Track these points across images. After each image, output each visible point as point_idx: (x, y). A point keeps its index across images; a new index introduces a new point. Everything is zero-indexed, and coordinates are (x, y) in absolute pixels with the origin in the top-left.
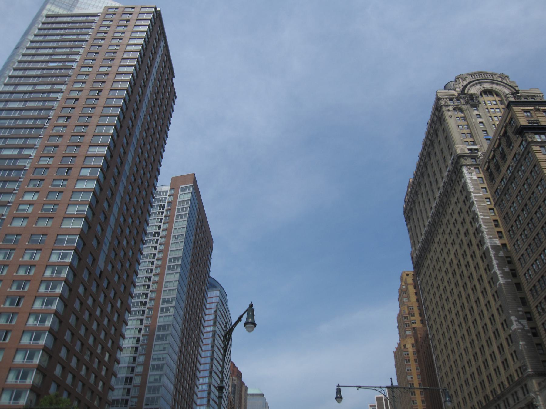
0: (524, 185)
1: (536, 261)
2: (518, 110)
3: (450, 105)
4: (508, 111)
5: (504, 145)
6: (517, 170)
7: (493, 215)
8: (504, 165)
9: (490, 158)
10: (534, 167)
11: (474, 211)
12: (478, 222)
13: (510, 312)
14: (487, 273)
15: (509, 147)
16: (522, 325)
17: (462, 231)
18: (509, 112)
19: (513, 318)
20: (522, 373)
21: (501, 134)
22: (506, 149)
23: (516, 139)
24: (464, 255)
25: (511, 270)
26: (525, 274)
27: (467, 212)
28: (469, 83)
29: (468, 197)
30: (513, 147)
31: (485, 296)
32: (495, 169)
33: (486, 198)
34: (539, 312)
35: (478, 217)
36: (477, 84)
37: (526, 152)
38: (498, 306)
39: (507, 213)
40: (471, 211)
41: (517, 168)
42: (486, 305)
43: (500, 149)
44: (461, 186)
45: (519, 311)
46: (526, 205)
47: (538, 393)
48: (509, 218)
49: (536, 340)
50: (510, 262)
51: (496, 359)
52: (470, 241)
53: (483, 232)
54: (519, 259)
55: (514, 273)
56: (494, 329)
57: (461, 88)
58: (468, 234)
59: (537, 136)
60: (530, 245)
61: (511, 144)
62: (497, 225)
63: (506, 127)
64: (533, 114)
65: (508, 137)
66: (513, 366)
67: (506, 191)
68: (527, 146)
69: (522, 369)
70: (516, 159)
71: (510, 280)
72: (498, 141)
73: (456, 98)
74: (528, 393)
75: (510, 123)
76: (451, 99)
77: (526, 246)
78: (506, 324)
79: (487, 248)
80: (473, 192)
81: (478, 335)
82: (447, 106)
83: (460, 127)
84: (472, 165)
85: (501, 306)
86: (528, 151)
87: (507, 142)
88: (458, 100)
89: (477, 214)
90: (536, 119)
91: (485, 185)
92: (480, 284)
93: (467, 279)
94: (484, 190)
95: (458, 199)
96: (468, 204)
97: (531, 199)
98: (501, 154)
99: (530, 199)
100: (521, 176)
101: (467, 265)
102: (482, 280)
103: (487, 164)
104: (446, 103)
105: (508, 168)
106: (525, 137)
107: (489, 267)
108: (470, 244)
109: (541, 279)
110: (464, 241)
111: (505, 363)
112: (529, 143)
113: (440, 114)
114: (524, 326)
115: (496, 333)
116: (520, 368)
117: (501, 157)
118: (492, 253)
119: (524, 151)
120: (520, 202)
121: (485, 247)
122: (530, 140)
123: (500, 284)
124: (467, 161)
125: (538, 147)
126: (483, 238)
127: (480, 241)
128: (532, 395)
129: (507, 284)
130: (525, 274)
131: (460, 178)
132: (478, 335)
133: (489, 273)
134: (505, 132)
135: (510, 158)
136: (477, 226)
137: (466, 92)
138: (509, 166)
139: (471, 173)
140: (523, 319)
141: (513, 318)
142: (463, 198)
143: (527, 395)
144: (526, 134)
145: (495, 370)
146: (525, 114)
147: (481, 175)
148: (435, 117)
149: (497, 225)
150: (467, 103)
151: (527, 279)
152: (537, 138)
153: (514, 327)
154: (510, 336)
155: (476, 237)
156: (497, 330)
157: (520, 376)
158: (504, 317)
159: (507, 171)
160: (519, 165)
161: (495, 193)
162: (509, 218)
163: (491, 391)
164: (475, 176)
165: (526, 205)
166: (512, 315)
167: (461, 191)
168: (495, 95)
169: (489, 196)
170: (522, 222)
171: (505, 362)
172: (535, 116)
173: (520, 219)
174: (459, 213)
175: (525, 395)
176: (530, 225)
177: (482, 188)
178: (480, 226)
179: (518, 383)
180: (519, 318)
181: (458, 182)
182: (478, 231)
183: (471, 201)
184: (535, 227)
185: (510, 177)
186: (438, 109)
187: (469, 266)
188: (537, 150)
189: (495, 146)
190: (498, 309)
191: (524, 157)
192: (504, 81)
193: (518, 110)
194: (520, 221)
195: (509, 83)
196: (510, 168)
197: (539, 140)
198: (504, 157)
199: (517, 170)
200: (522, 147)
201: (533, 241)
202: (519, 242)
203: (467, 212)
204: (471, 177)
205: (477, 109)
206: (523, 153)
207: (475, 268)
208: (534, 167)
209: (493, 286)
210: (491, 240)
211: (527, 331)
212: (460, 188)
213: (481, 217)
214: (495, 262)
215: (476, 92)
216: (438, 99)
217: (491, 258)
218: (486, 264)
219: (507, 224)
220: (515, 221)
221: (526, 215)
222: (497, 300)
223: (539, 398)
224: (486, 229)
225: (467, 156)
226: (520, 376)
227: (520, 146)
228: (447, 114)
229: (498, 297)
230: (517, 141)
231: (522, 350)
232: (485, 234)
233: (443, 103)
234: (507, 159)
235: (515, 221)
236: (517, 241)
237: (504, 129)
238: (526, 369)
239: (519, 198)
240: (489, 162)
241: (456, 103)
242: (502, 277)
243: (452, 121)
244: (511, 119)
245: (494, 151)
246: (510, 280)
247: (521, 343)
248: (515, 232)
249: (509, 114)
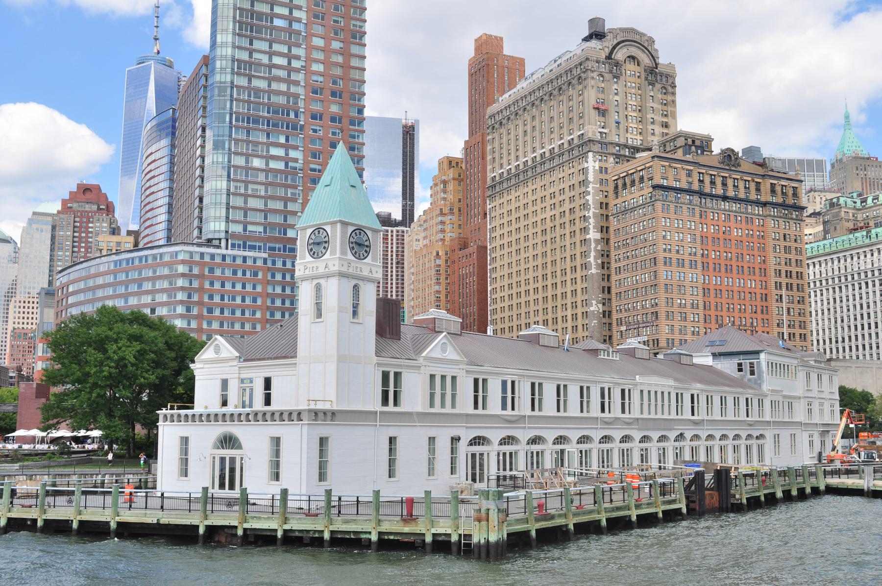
19: (594, 302)
80: (593, 183)
118: (593, 245)
121: (588, 237)
141: (594, 302)
180: (598, 302)
214: (593, 254)
232: (591, 227)
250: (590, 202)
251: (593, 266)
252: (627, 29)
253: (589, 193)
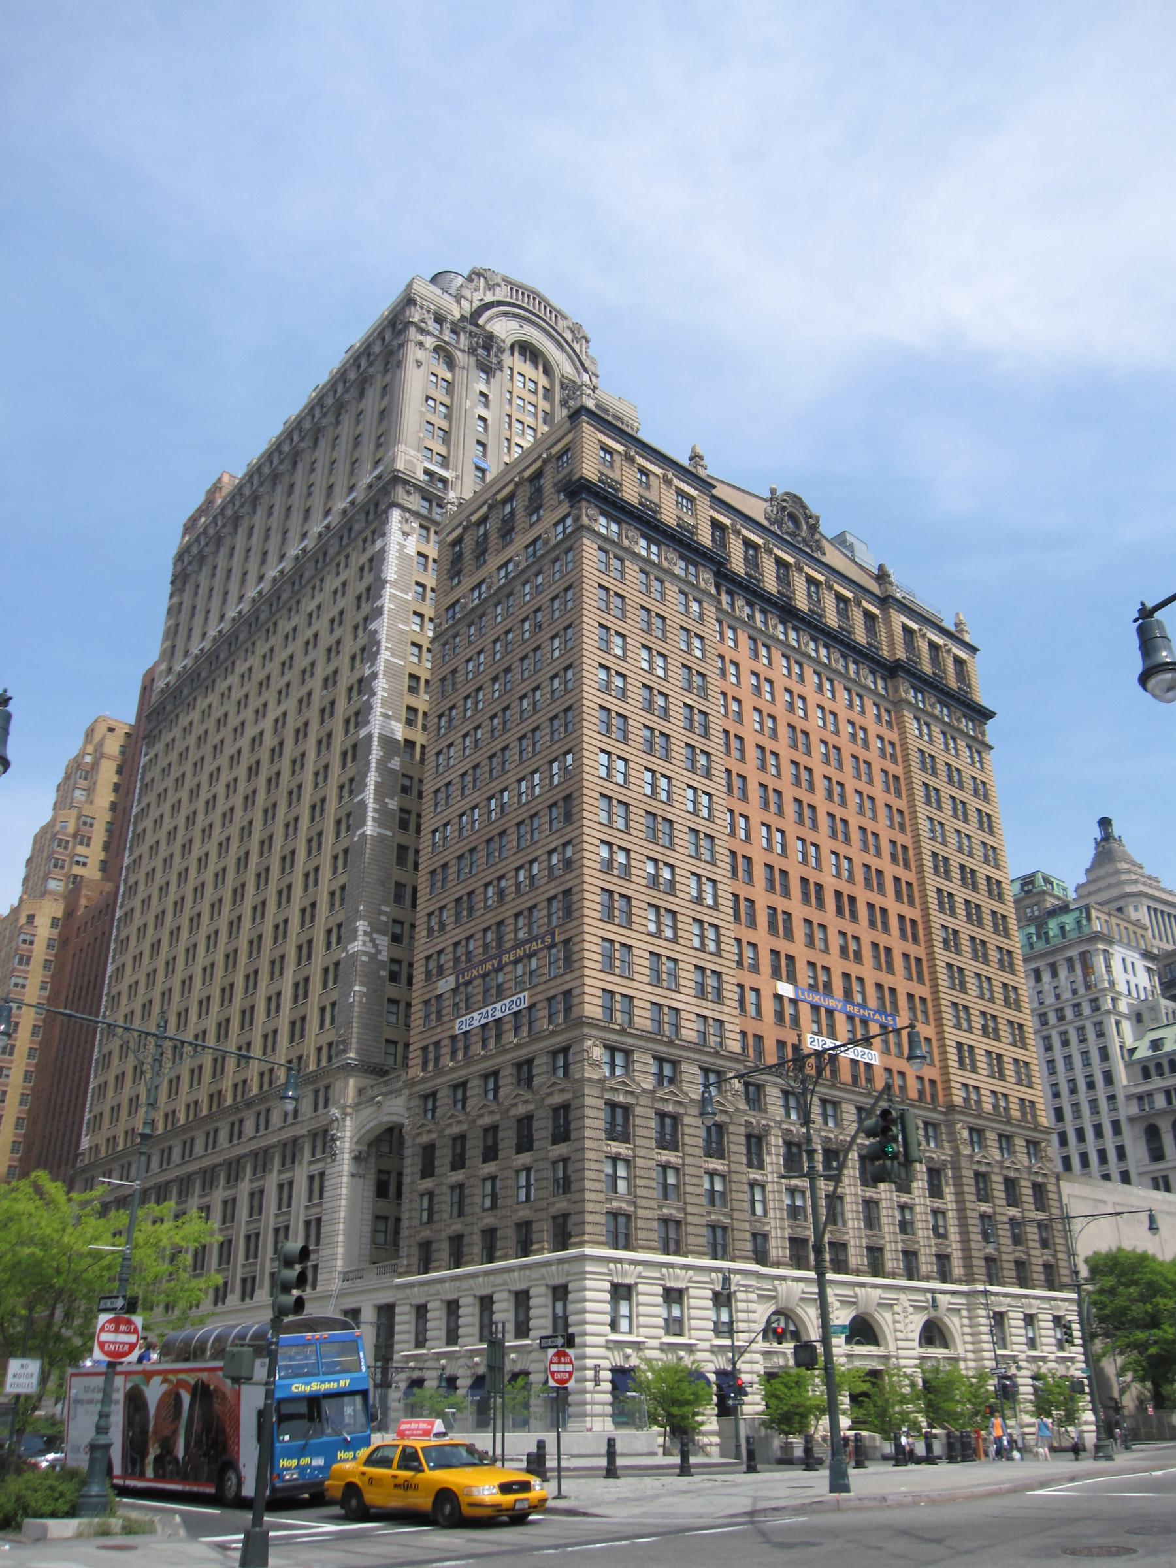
0: (523, 621)
1: (473, 808)
2: (591, 437)
3: (428, 333)
4: (568, 425)
5: (520, 504)
6: (524, 577)
7: (410, 662)
8: (498, 552)
9: (474, 518)
10: (567, 590)
11: (376, 632)
12: (373, 665)
14: (341, 797)
15: (531, 515)
16: (375, 946)
17: (321, 672)
19: (362, 925)
20: (330, 1059)
21: (527, 474)
22: (520, 513)
23: (555, 503)
24: (301, 732)
25: (402, 810)
26: (434, 832)
27: (356, 627)
28: (500, 303)
29: (373, 591)
30: (539, 519)
31: (314, 853)
32: (473, 551)
33: (416, 613)
34: (430, 930)
35: (378, 652)
36: (515, 315)
37: (564, 546)
38: (335, 886)
39: (454, 672)
40: (365, 629)
41: (524, 577)
42: (307, 875)
43: (508, 509)
44: (368, 554)
45: (381, 913)
46: (507, 670)
47: (349, 1110)
48: (454, 684)
49: (392, 991)
50: (405, 790)
51: (278, 1011)
52: (332, 703)
53: (374, 694)
54: (437, 791)
55: (406, 820)
56: (304, 939)
57: (476, 304)
58: (335, 683)
59: (603, 521)
60: (475, 767)
61: (537, 509)
62: (412, 690)
63: (545, 462)
64: (617, 464)
65: (539, 490)
66: (314, 1035)
67: (476, 616)
68: (573, 532)
69: (333, 1049)
70: (535, 552)
71: (389, 833)
72: (511, 487)
73: (453, 323)
74: (326, 1105)
75: (560, 457)
76: (439, 319)
77: (466, 765)
78: (339, 933)
79: (370, 736)
80: (394, 584)
81: (255, 943)
82: (423, 331)
83: (431, 403)
84: (416, 514)
85: (343, 888)
86: (569, 546)
87: (530, 499)
88: (453, 331)
89: (378, 643)
90: (618, 478)
91: (430, 580)
92: (313, 819)
93: (285, 794)
94: (420, 590)
95: (344, 584)
96: (366, 608)
97: (526, 662)
98: (503, 521)
99: (522, 659)
100: (528, 598)
101: (298, 762)
102: (322, 811)
103: (459, 530)
104: (423, 320)
105: (506, 564)
106: (580, 509)
107: (353, 785)
108: (328, 711)
109: (467, 855)
110: (316, 698)
111: (298, 1027)
112: (583, 526)
113: (395, 343)
114: (379, 952)
115: (305, 950)
116: (330, 1045)
117: (499, 530)
118: (376, 753)
119: (562, 541)
120: (498, 656)
121: (363, 733)
122: (585, 521)
123: (363, 835)
124: (411, 498)
125: (595, 546)
126: (369, 707)
127: (357, 714)
128: (335, 1112)
129: (380, 839)
130: (434, 832)
131: (374, 532)
132: (255, 943)
133: (346, 799)
134: (539, 474)
135: (520, 541)
136: (367, 672)
137: (481, 322)
138: (510, 560)
139: (406, 534)
140: (384, 933)
141: (362, 925)
142: (362, 587)
143: (321, 1111)
144: (584, 504)
145: (265, 1036)
146: (602, 454)
147: (432, 551)
148: (379, 342)
149: (412, 690)
150: (472, 351)
151: (434, 844)
152: (602, 525)
153: (357, 946)
154: (337, 964)
155: (350, 699)
156: (310, 942)
157: (324, 1063)
158: (340, 917)
159: (499, 569)
160: (534, 569)
161: (447, 609)
162: (454, 684)
163: (236, 1086)
164: (412, 545)
165: (507, 670)
166: (364, 918)
167: (362, 569)
168: (541, 368)
169: (428, 612)
170: (480, 706)
171: (298, 1025)
172: (618, 471)
173: (480, 697)
174: (332, 621)
175: (315, 1110)
176: (496, 721)
177: (418, 584)
178: (374, 676)
179: (313, 1078)
180: (376, 928)
181: (365, 541)
182: (363, 686)
183: (378, 603)
184: (505, 730)
185: (500, 588)
186: (394, 330)
187: (302, 766)
188: (590, 550)
189: (499, 497)
190: (332, 894)
191: (554, 555)
192: (577, 347)
193: (591, 437)
194: (477, 703)
195: (584, 358)
196: (511, 567)
197: (603, 531)
198: (507, 530)
199: (524, 577)
200: (560, 528)
201: (486, 762)
202: (452, 750)
203: (356, 627)
204: (403, 544)
205: (488, 381)
206: (558, 544)
207: (316, 774)
208: (567, 590)
209: (343, 834)
210: (385, 721)
211: (381, 965)
212: (364, 559)
213: (384, 655)
214: (372, 778)
215: (503, 337)
216: (409, 301)
217: (368, 763)
218: (350, 773)
219: (444, 697)
220: (466, 698)
221: (497, 695)
222: (340, 870)
223: (348, 1123)
224: (384, 689)
225: (415, 486)
226: (324, 1063)
227: (556, 525)
228: (413, 353)
229: (345, 866)
230: (555, 507)
231: (352, 1005)
232: (377, 701)
233: (416, 319)
234: (512, 541)
235: (466, 698)
236: (451, 745)
237: (539, 463)
238: (344, 1051)
239: (498, 646)
240: (466, 529)
241: (447, 336)
242: (374, 819)
243: (419, 376)
244: (566, 451)
245: (490, 507)
246: (389, 833)
247: (357, 988)
248: (454, 723)
249: (566, 434)
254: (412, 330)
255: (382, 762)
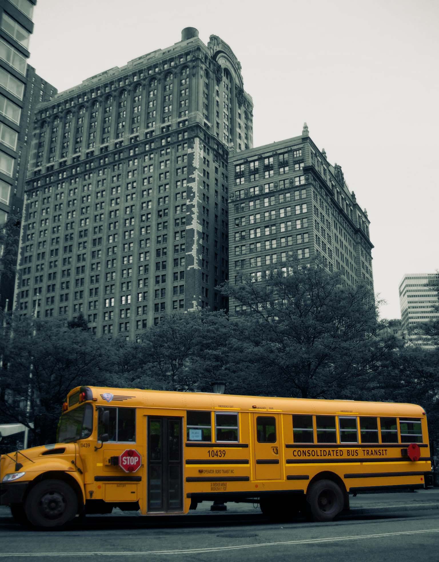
13: (194, 296)
18: (302, 144)
19: (195, 303)
36: (225, 57)
45: (199, 298)
57: (215, 51)
118: (196, 237)
121: (188, 227)
141: (195, 303)
150: (214, 72)
166: (195, 300)
214: (195, 247)
232: (195, 217)
242: (197, 263)
250: (195, 189)
251: (196, 261)
252: (225, 44)
253: (193, 180)
254: (200, 62)
255: (198, 241)
